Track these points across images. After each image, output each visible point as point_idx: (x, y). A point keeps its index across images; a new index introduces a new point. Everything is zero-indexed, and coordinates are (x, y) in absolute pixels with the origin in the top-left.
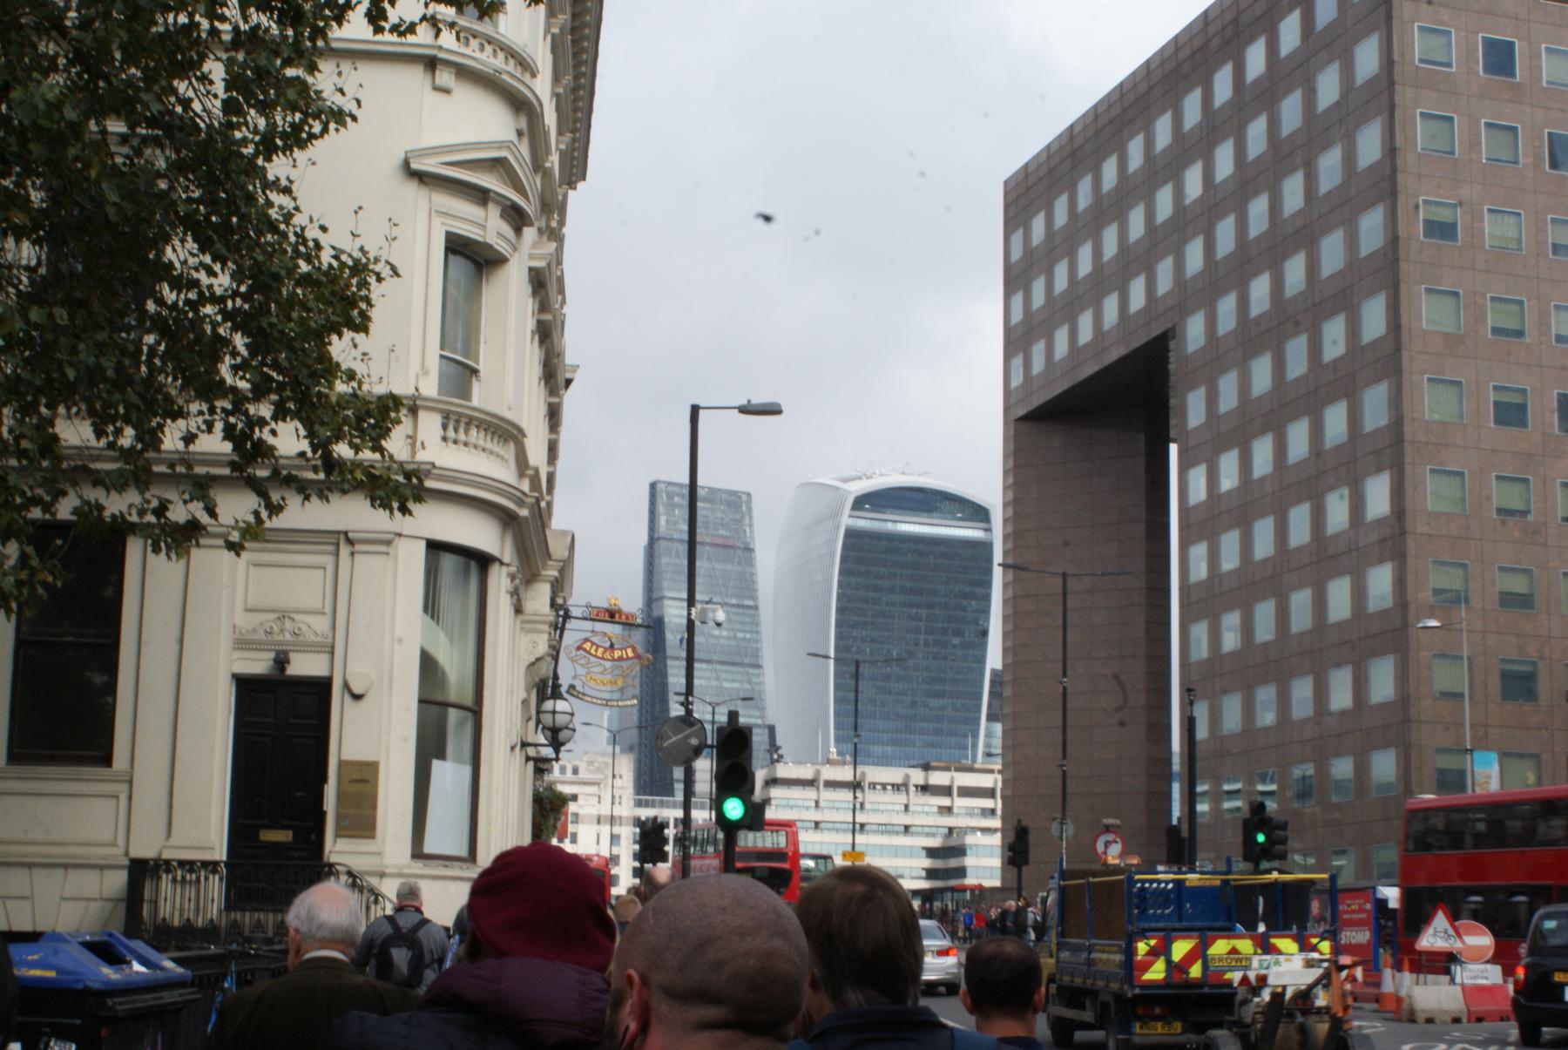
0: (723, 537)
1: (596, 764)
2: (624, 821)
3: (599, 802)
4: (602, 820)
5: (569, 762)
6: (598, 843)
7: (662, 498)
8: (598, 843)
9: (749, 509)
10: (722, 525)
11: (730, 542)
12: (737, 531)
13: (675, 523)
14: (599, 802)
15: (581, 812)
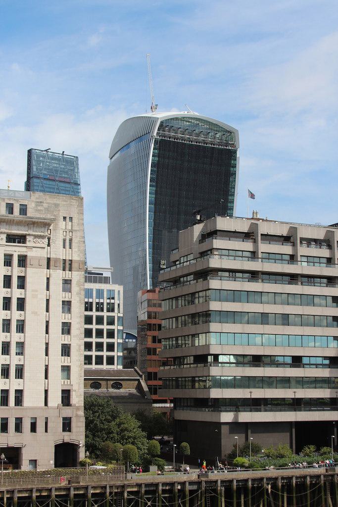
0: (65, 178)
1: (45, 205)
2: (74, 265)
3: (49, 245)
4: (52, 263)
5: (17, 201)
6: (48, 289)
7: (34, 157)
8: (48, 289)
9: (77, 164)
10: (64, 172)
11: (68, 180)
12: (71, 175)
13: (41, 170)
14: (49, 245)
15: (30, 254)
